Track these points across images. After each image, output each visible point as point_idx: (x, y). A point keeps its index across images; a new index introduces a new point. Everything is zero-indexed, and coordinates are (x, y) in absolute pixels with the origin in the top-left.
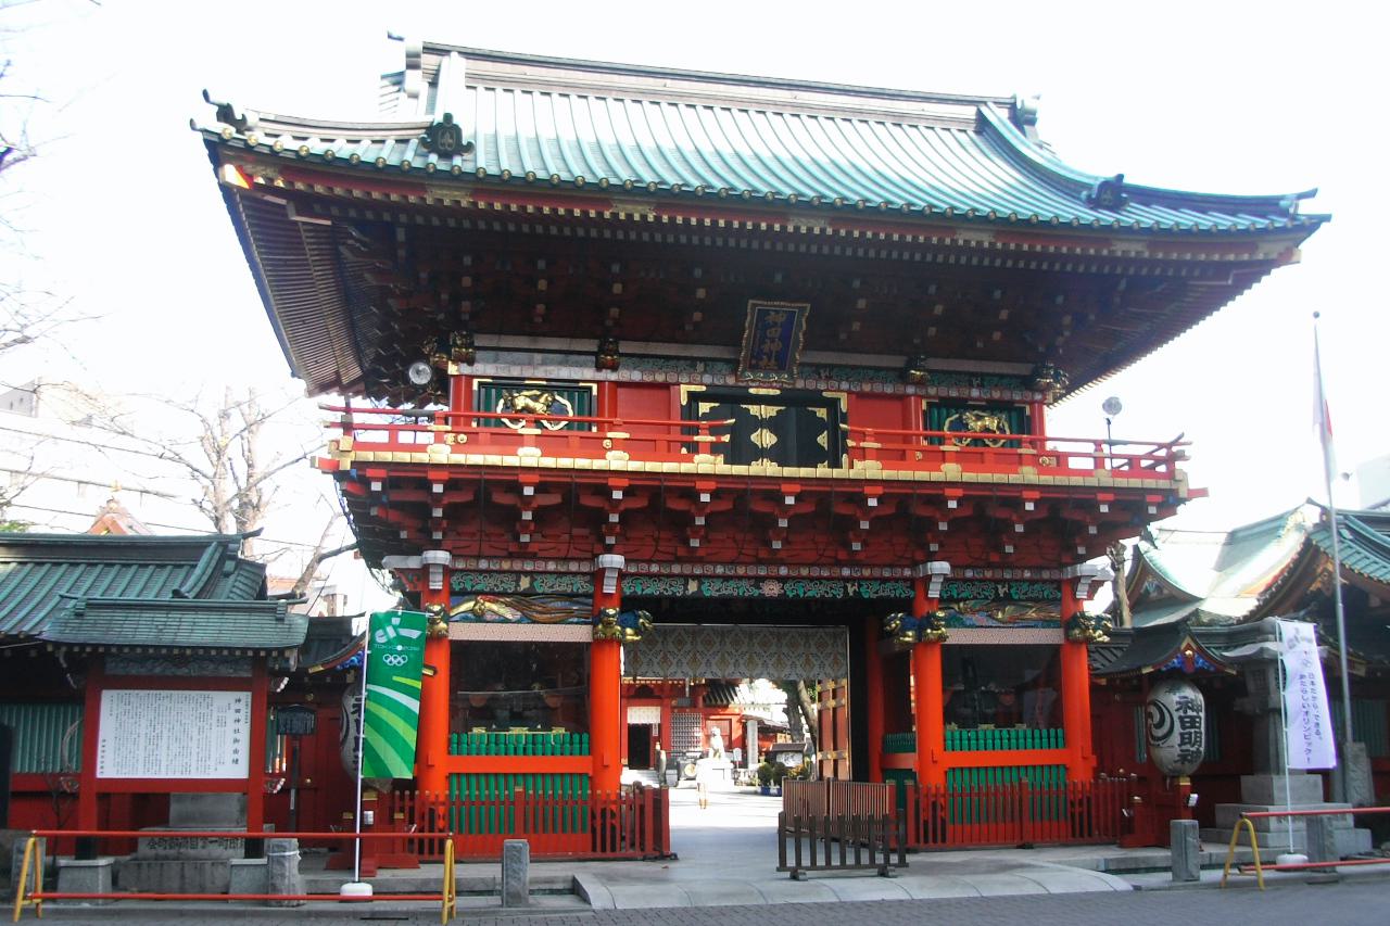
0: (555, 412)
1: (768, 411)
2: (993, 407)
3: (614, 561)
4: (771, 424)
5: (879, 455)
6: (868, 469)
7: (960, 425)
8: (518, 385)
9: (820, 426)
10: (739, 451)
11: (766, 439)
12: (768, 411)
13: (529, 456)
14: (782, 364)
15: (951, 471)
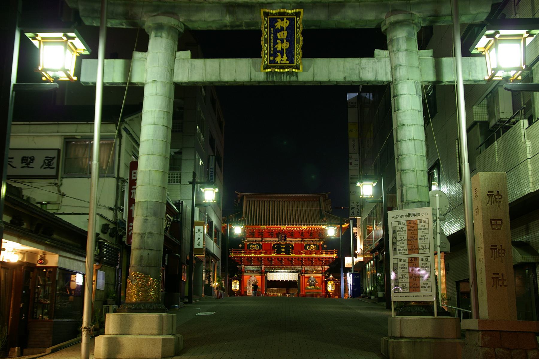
0: (257, 247)
1: (284, 246)
2: (314, 245)
3: (263, 266)
4: (284, 248)
5: (294, 253)
6: (294, 255)
7: (309, 248)
8: (252, 244)
9: (290, 248)
10: (279, 252)
11: (283, 250)
12: (284, 246)
13: (253, 255)
14: (285, 240)
15: (304, 255)
